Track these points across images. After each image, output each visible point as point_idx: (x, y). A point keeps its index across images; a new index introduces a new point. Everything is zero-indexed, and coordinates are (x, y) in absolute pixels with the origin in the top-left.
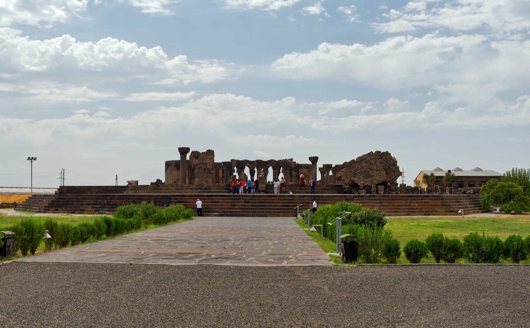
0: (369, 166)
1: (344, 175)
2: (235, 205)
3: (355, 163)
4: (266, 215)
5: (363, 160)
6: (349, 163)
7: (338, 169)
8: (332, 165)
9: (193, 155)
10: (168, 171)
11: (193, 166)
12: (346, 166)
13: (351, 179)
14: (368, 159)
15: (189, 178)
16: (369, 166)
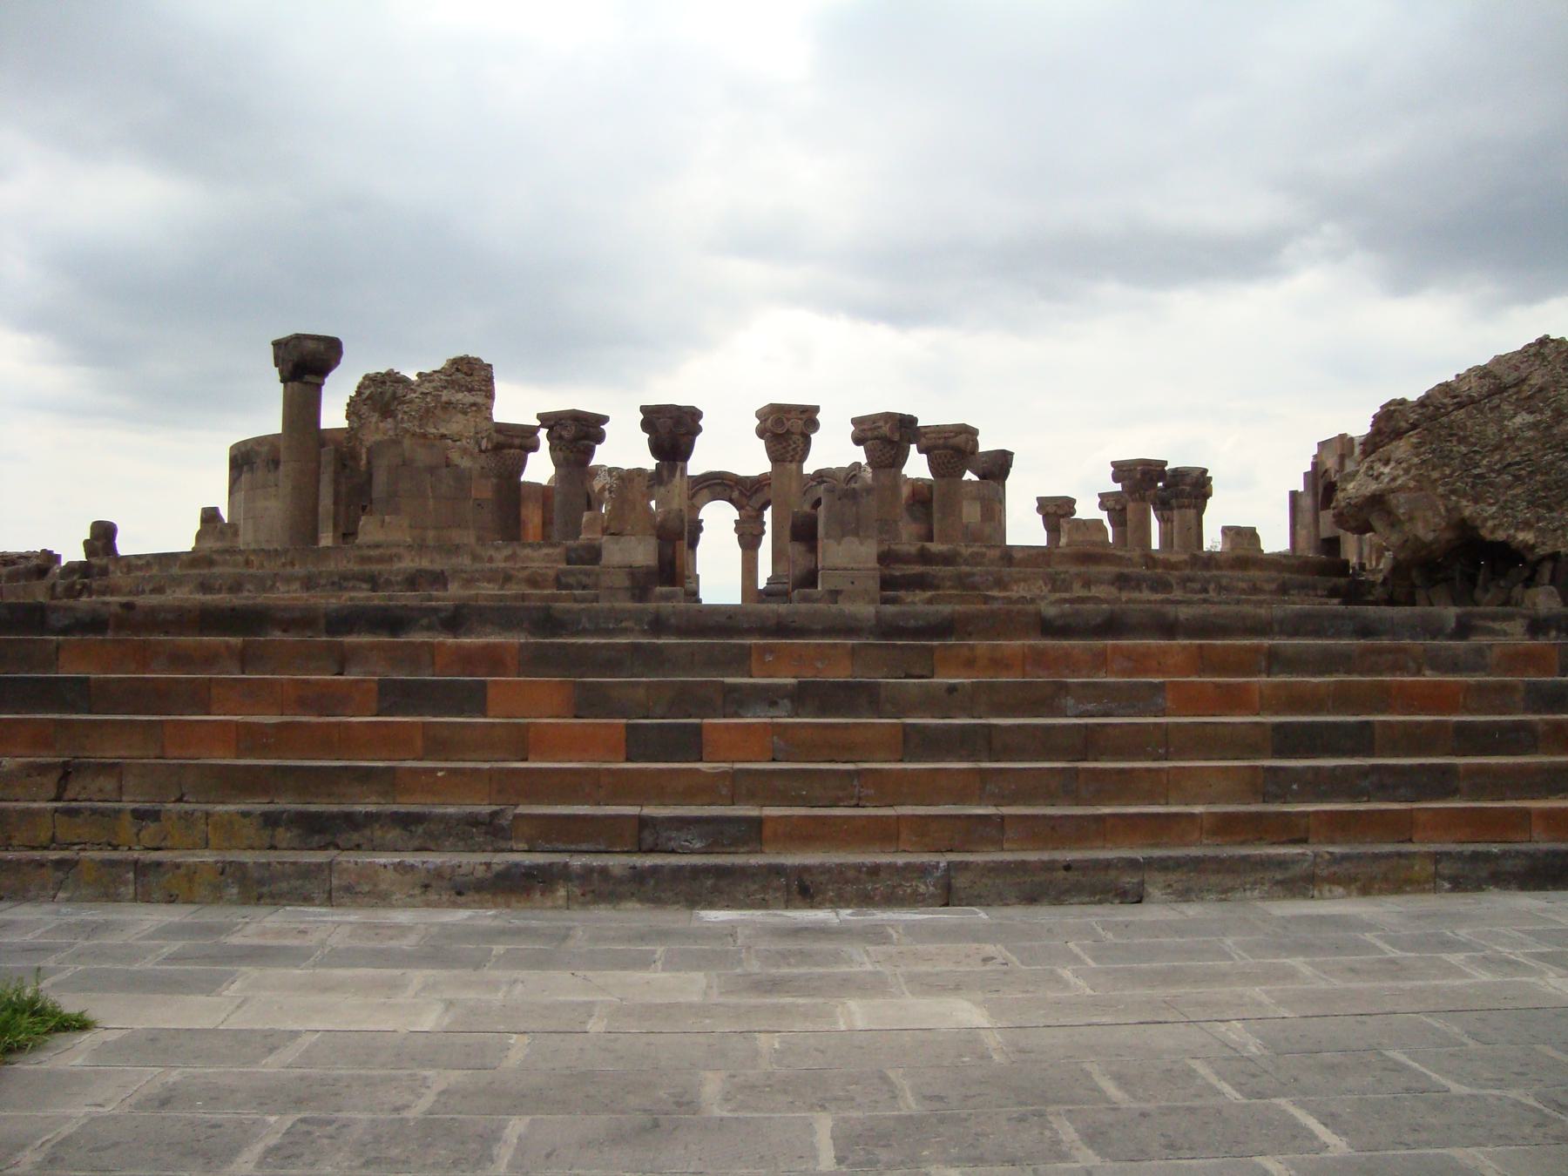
0: (1549, 427)
1: (1412, 484)
2: (691, 744)
3: (1460, 406)
4: (1129, 880)
5: (1506, 388)
6: (1423, 403)
7: (1188, 488)
8: (1165, 463)
9: (367, 392)
10: (240, 496)
11: (364, 457)
12: (1403, 425)
13: (1457, 508)
14: (1536, 380)
15: (342, 530)
16: (1549, 427)
